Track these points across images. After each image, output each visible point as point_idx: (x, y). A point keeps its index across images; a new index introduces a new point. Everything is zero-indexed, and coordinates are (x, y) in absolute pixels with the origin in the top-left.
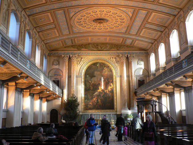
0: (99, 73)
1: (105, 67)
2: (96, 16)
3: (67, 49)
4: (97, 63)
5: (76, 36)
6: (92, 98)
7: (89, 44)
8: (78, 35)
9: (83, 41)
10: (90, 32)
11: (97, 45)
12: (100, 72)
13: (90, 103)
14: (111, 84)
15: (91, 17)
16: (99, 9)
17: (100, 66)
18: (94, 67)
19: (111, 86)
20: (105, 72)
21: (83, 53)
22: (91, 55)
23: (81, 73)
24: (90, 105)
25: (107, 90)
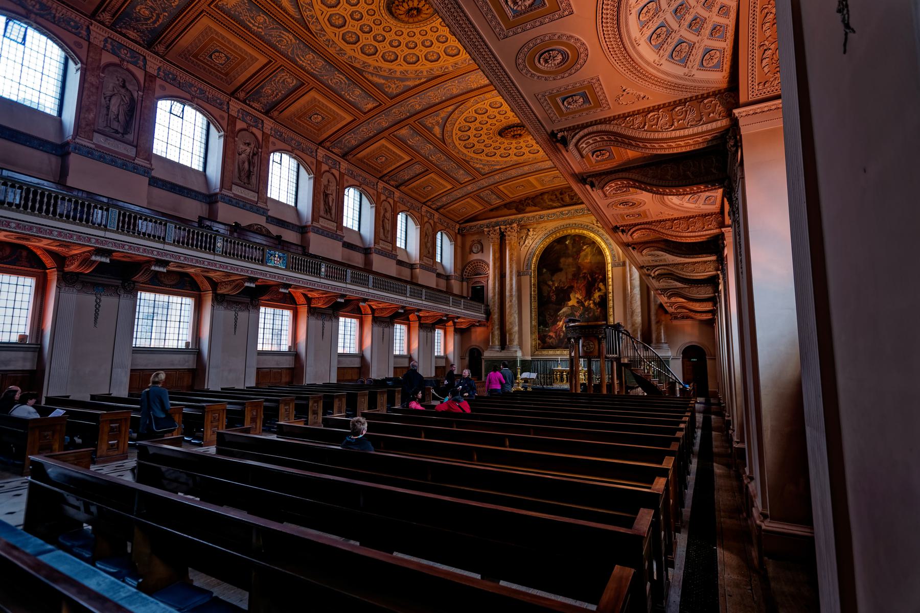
0: (570, 260)
1: (584, 244)
2: (494, 121)
3: (494, 213)
4: (564, 238)
5: (491, 180)
6: (555, 322)
7: (542, 194)
8: (497, 178)
9: (521, 193)
10: (517, 165)
11: (561, 194)
12: (573, 257)
13: (551, 334)
14: (601, 286)
15: (485, 127)
16: (487, 102)
17: (572, 244)
18: (558, 247)
19: (600, 290)
20: (586, 256)
21: (528, 218)
22: (551, 221)
23: (529, 266)
24: (552, 337)
25: (591, 302)
